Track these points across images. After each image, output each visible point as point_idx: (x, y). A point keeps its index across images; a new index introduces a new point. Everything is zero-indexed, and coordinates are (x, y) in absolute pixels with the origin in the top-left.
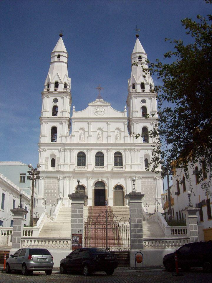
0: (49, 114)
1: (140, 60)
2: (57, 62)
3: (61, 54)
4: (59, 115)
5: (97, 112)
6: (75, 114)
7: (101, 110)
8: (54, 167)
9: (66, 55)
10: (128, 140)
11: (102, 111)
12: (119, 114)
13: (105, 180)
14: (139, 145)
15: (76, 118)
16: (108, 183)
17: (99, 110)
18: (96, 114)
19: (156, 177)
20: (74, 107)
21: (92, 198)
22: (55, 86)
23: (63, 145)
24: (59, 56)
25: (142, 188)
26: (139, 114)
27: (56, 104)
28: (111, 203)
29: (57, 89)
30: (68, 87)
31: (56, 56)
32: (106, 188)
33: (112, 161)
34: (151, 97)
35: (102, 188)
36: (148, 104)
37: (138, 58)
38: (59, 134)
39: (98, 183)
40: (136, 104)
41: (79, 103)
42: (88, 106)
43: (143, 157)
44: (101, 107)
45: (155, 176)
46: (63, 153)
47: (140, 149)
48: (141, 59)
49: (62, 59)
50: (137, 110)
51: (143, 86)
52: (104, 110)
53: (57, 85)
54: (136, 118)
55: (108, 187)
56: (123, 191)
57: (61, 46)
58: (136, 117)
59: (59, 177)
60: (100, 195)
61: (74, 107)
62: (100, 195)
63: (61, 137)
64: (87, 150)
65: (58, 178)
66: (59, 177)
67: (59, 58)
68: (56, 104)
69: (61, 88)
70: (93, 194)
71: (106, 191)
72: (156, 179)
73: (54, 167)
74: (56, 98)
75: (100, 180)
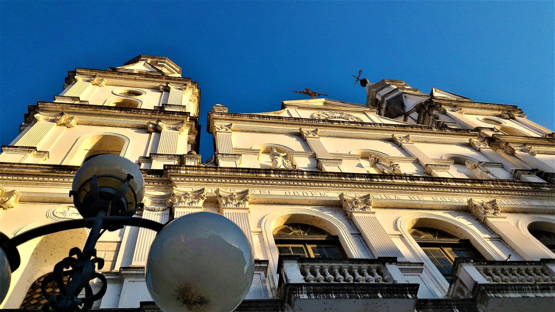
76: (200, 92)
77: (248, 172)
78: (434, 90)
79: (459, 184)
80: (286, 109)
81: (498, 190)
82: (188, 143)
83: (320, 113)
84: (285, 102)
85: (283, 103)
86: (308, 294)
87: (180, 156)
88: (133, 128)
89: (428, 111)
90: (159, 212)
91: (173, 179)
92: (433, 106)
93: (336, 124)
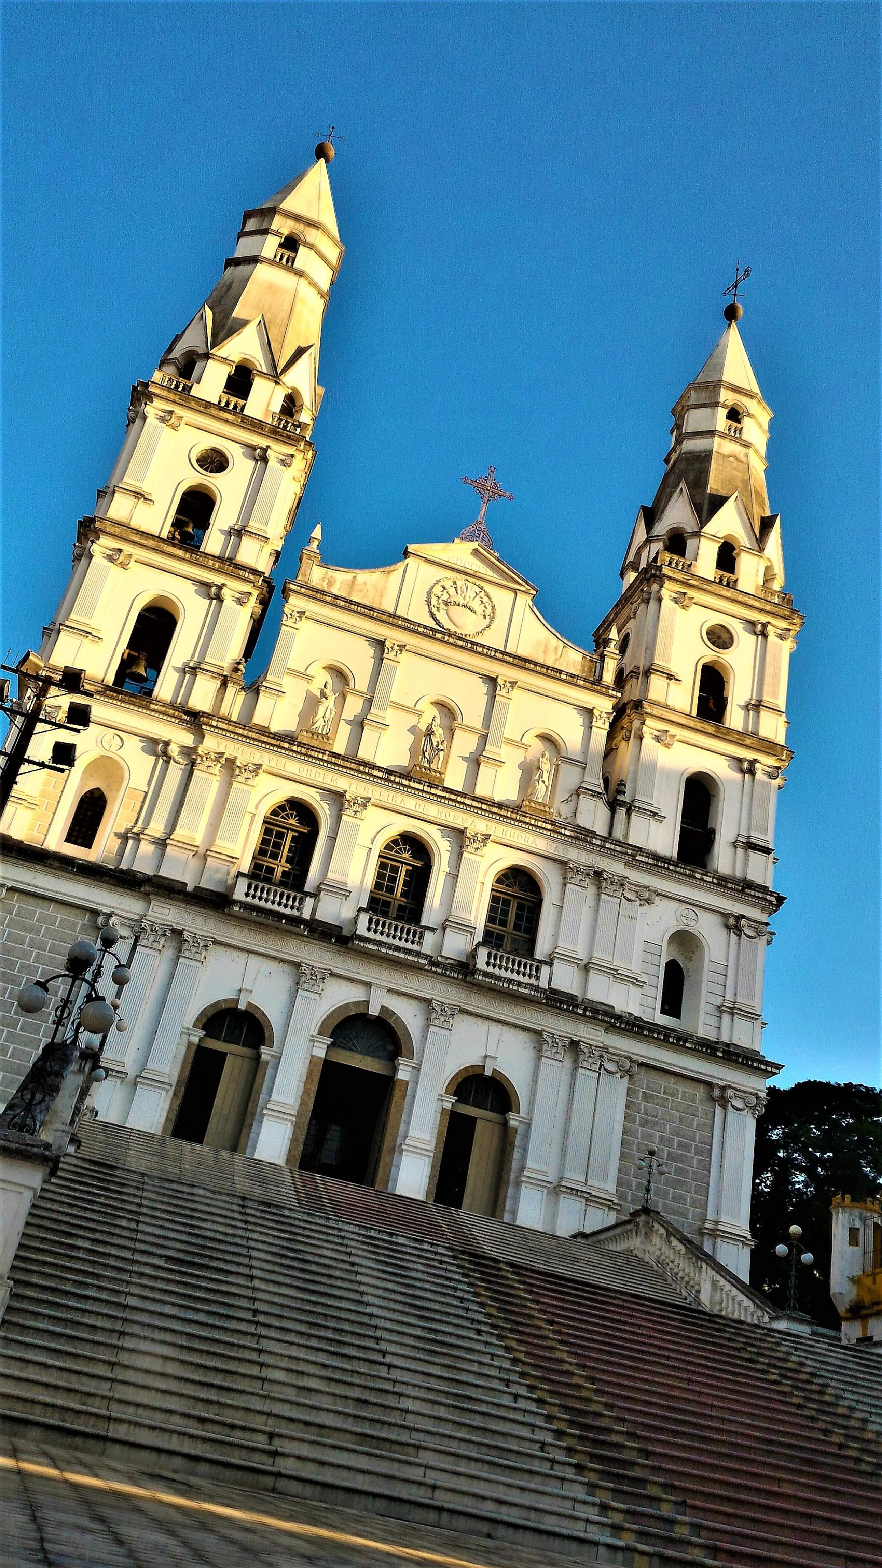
0: (158, 517)
1: (735, 424)
2: (272, 262)
3: (312, 235)
4: (213, 542)
5: (446, 603)
6: (316, 574)
7: (476, 604)
8: (89, 846)
9: (333, 253)
10: (594, 815)
11: (479, 609)
12: (573, 659)
13: (408, 1015)
14: (658, 863)
15: (317, 594)
16: (424, 1037)
17: (462, 602)
18: (441, 616)
19: (724, 1089)
20: (317, 533)
21: (294, 1112)
22: (227, 386)
23: (195, 720)
24: (291, 244)
25: (625, 1132)
26: (683, 695)
27: (216, 482)
28: (412, 1175)
29: (241, 402)
30: (305, 417)
31: (277, 234)
32: (403, 1074)
33: (477, 913)
34: (765, 625)
35: (370, 1064)
36: (739, 661)
37: (722, 413)
38: (180, 650)
39: (356, 1027)
40: (680, 636)
41: (350, 525)
42: (406, 554)
43: (665, 944)
44: (478, 590)
45: (715, 1081)
46: (175, 773)
47: (655, 892)
48: (739, 422)
49: (304, 258)
50: (674, 669)
51: (727, 557)
52: (489, 611)
53: (240, 381)
54: (667, 707)
55: (417, 1069)
56: (505, 1124)
57: (313, 195)
58: (661, 700)
59: (109, 916)
60: (351, 1111)
61: (317, 533)
62: (351, 1111)
63: (192, 670)
64: (337, 798)
65: (100, 920)
66: (109, 916)
67: (287, 253)
68: (216, 482)
69: (264, 399)
70: (306, 1091)
71: (397, 1093)
72: (724, 1102)
73: (89, 846)
74: (215, 450)
75: (374, 1011)
76: (314, 456)
77: (274, 738)
78: (736, 494)
79: (475, 804)
80: (406, 561)
81: (513, 819)
82: (251, 617)
83: (448, 584)
84: (412, 548)
85: (407, 548)
86: (240, 909)
87: (224, 676)
88: (195, 581)
89: (648, 580)
90: (183, 767)
91: (204, 727)
92: (657, 576)
93: (439, 636)
